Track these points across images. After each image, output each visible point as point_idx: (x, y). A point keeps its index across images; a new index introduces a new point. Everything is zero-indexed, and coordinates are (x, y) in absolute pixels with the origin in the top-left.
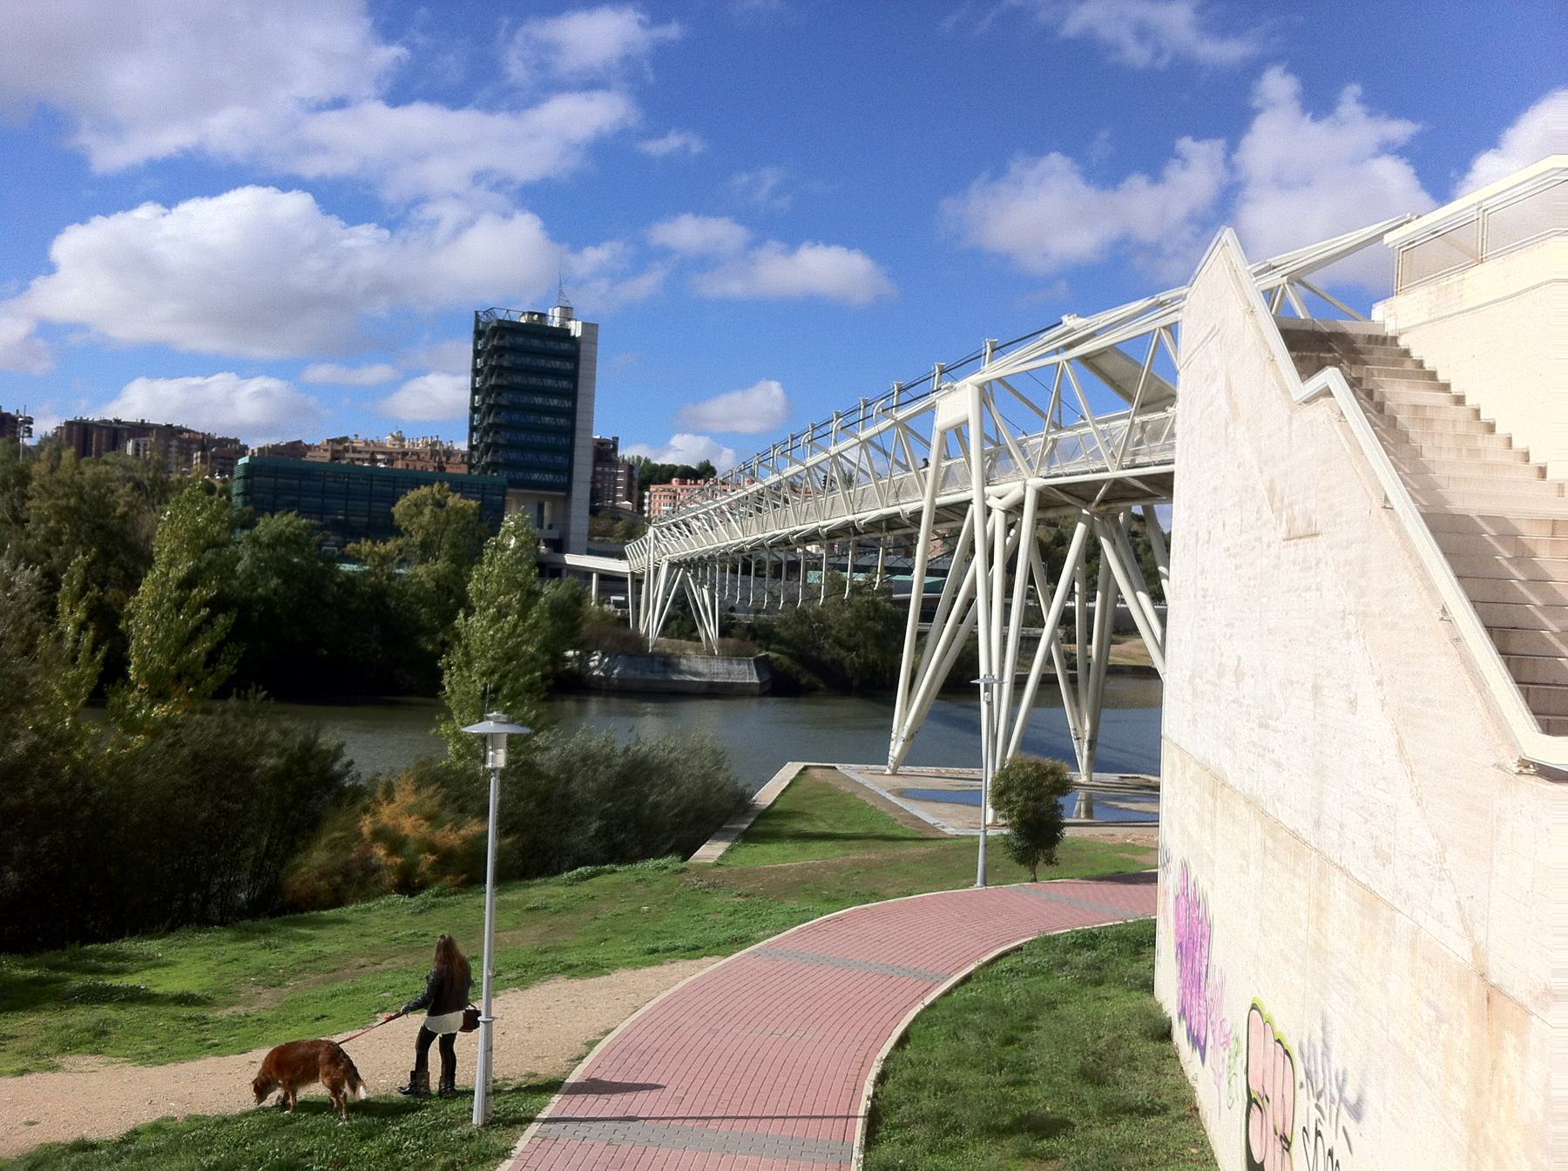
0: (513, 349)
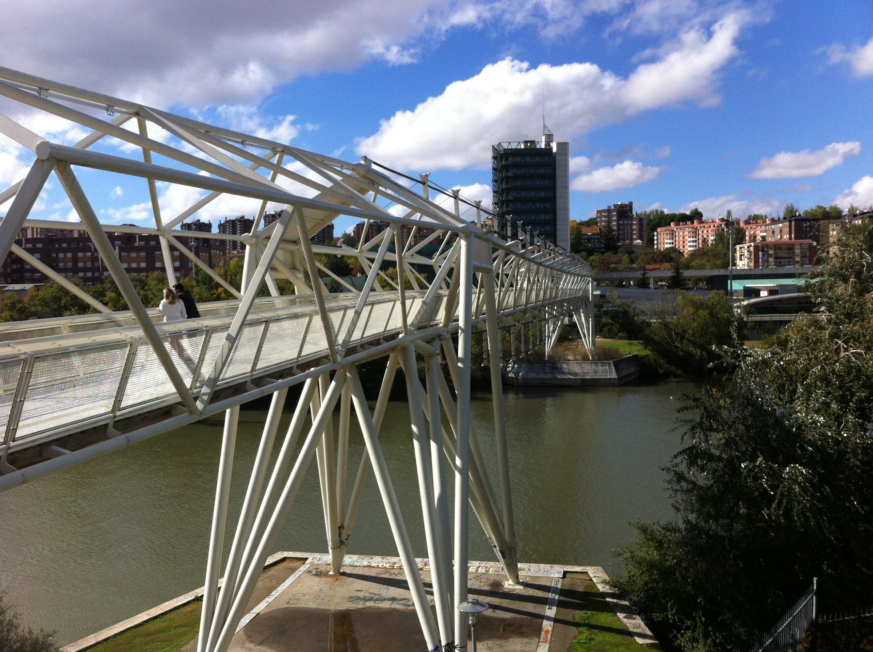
0: (514, 165)
